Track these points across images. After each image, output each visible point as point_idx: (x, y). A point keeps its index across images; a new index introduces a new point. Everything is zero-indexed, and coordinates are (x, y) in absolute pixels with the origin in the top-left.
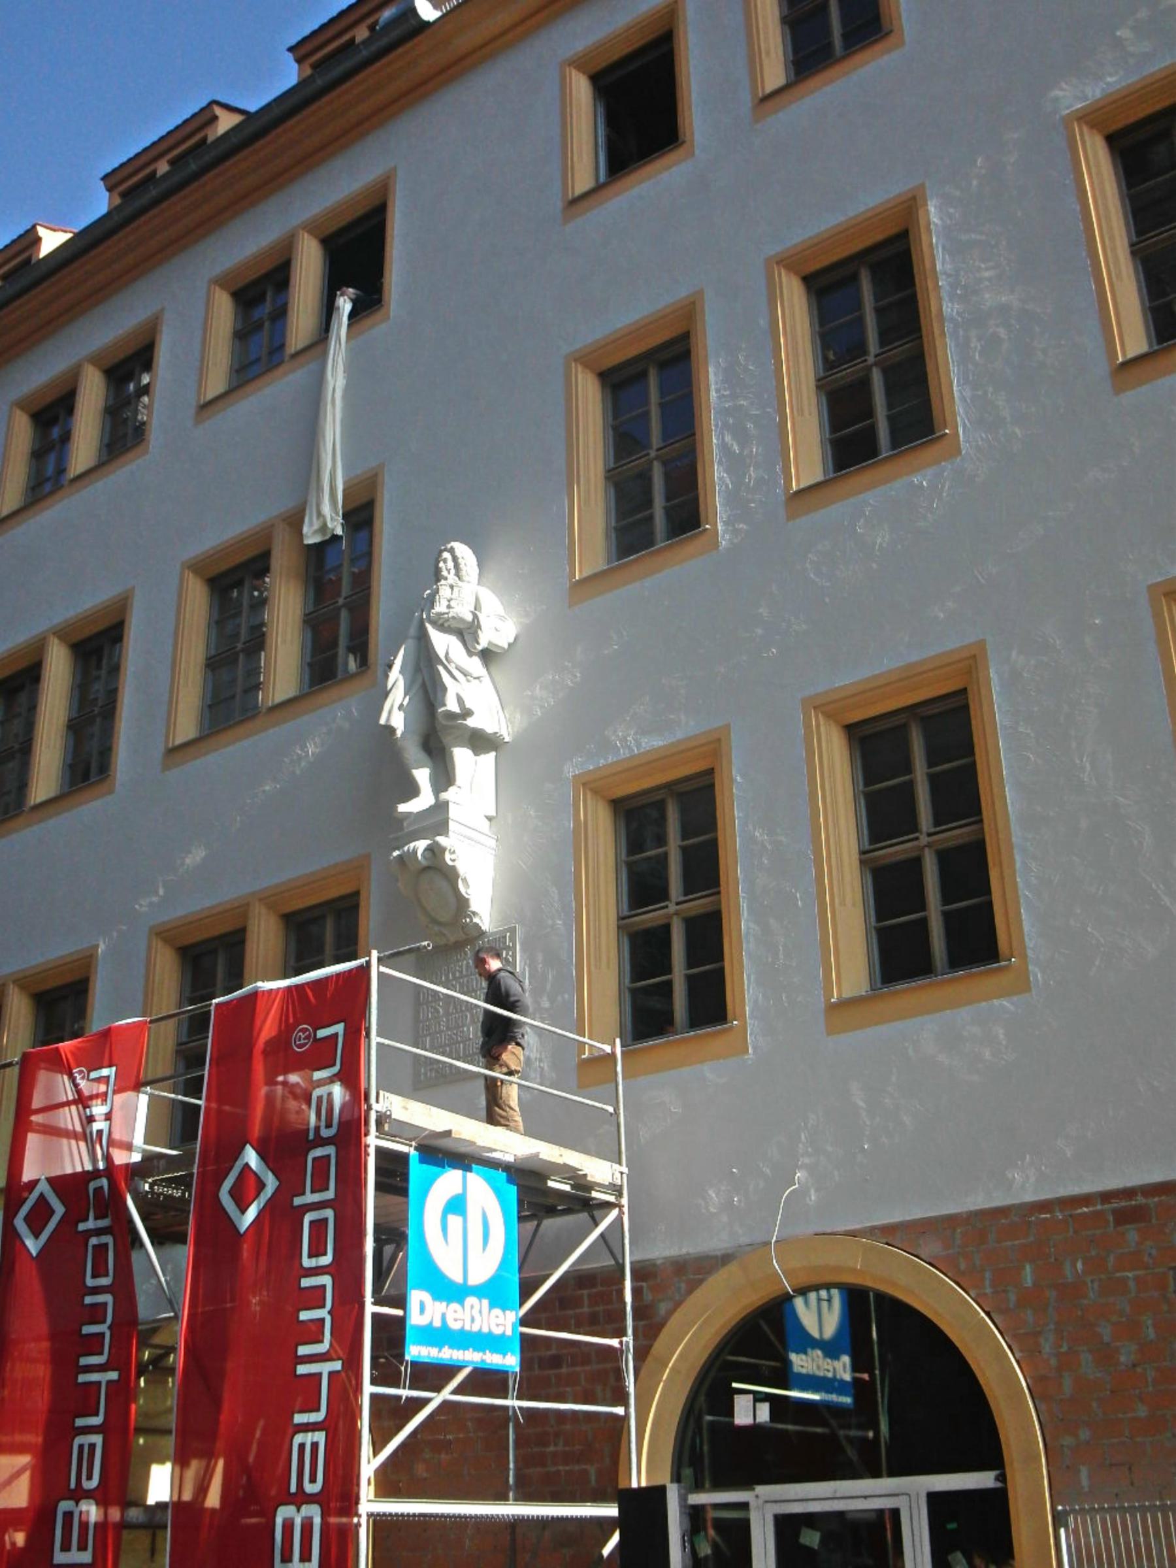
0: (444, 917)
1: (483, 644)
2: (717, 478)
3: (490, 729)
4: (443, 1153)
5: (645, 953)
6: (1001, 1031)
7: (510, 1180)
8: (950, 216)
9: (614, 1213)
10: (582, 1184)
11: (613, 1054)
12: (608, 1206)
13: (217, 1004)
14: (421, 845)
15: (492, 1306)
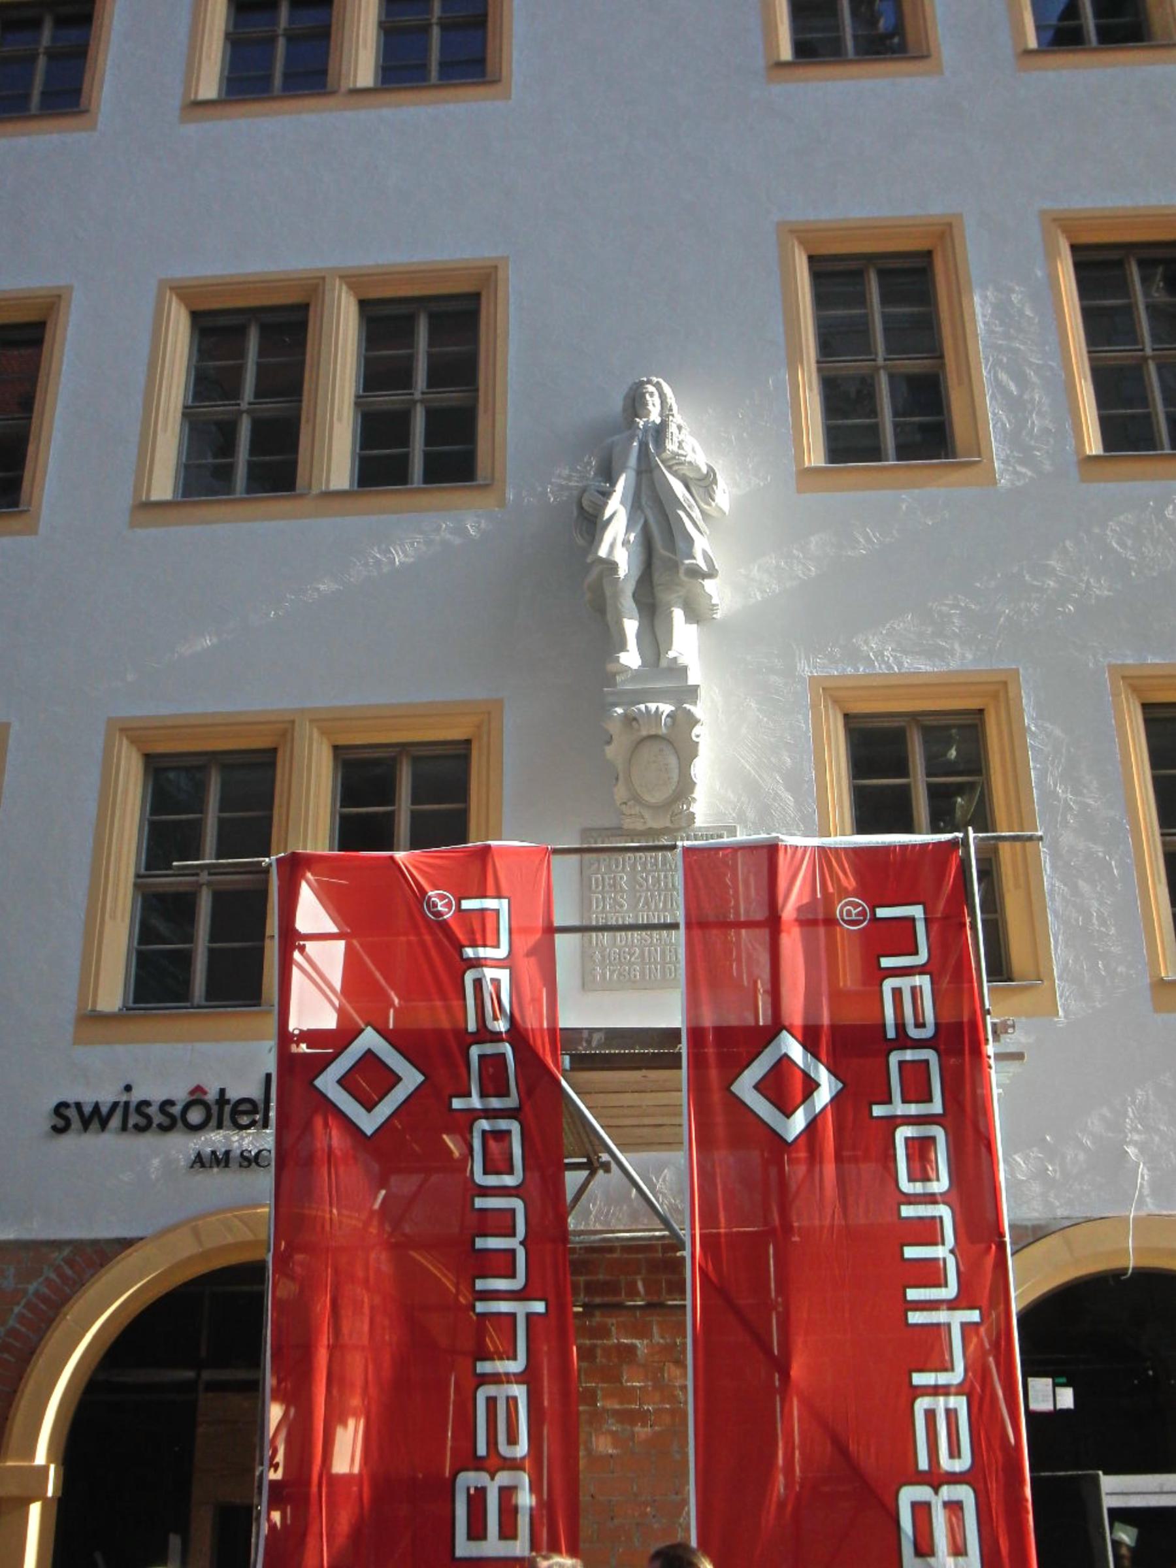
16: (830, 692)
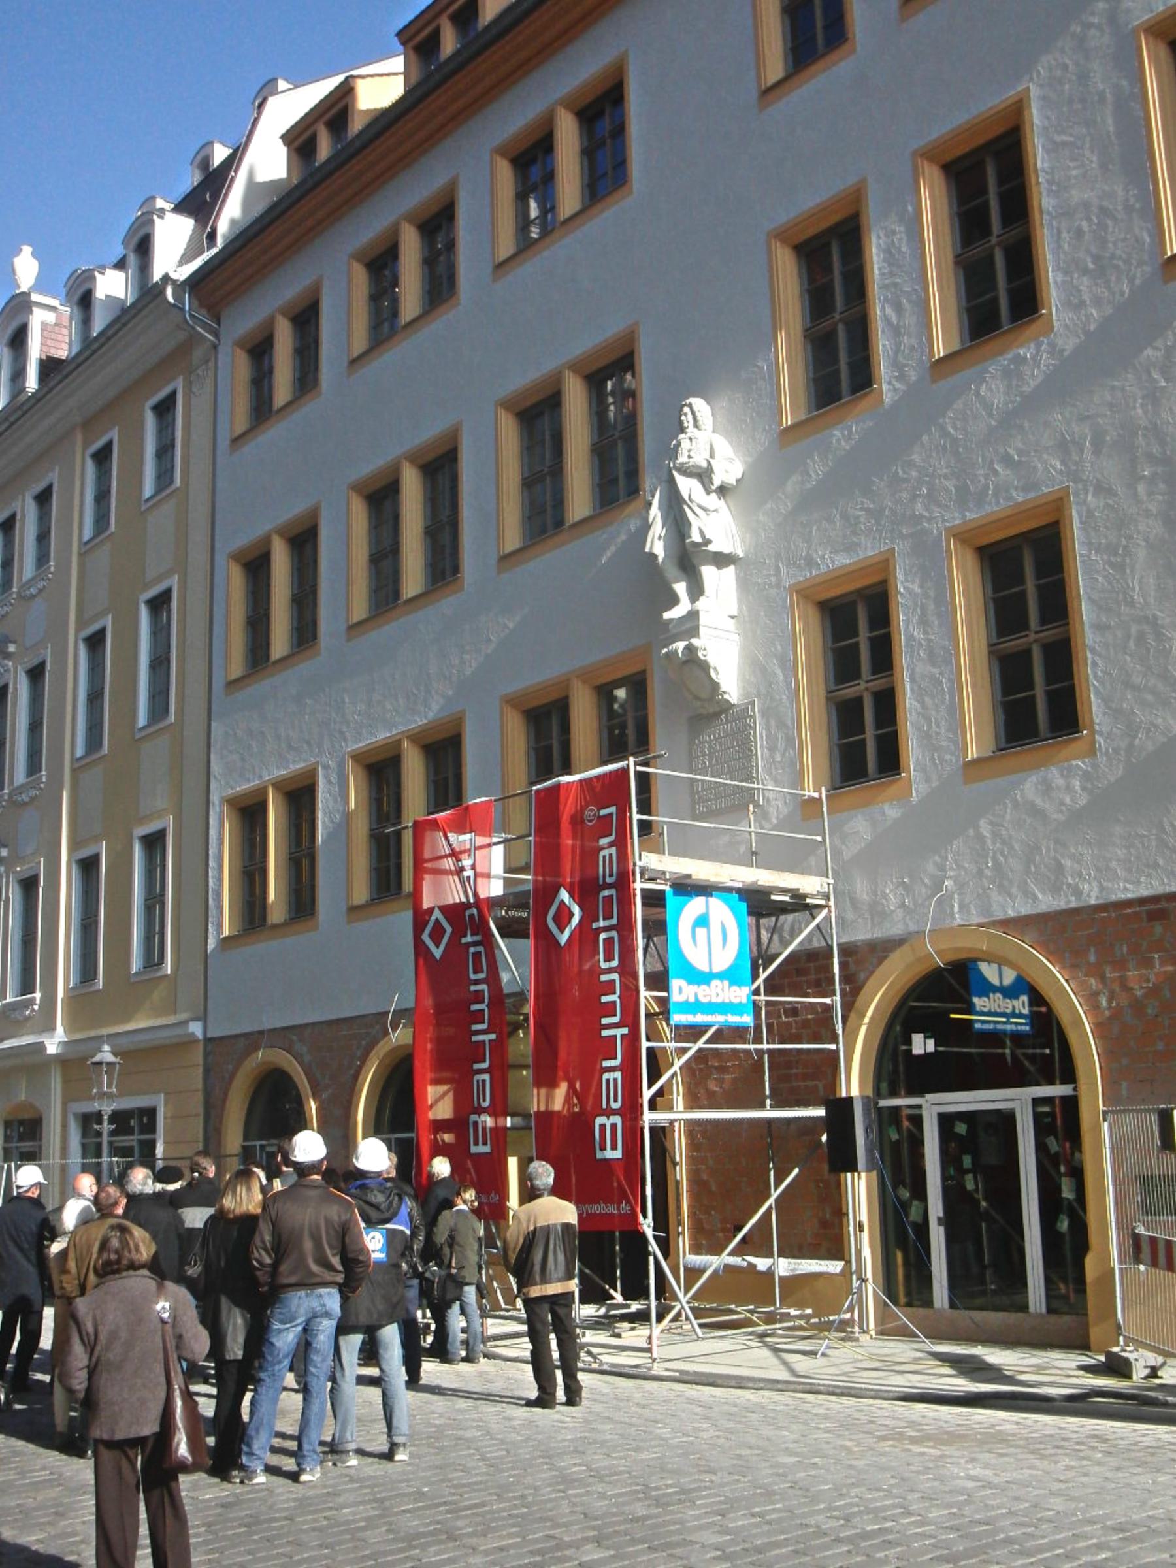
0: (703, 695)
1: (717, 483)
2: (882, 344)
3: (726, 551)
4: (686, 887)
5: (846, 717)
6: (1078, 783)
7: (741, 899)
8: (1048, 118)
9: (825, 911)
10: (797, 895)
11: (820, 799)
12: (820, 907)
13: (537, 791)
14: (680, 646)
15: (731, 984)
16: (803, 592)
